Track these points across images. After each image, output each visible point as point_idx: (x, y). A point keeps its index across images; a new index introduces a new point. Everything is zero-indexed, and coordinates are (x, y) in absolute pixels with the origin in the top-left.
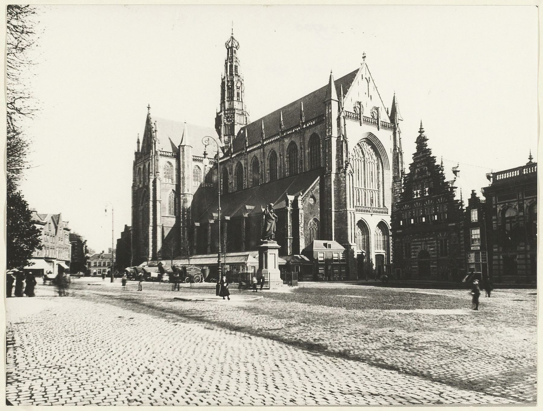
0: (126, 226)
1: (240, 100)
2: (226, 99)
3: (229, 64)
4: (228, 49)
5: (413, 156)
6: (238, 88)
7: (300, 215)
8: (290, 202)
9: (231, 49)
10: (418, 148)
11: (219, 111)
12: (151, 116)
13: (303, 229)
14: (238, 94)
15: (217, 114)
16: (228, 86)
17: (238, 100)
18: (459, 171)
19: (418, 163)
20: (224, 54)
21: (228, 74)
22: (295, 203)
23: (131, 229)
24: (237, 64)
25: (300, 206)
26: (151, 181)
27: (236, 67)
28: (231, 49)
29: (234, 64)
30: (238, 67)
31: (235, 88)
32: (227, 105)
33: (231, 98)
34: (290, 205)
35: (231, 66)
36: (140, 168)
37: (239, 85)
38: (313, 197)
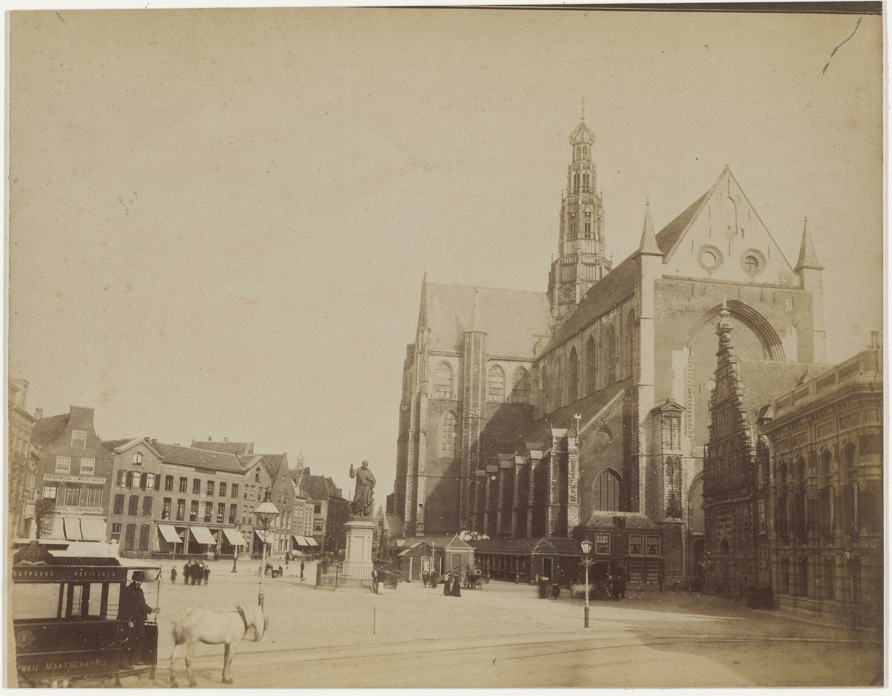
1: (592, 236)
3: (573, 173)
4: (574, 146)
6: (588, 215)
7: (570, 464)
8: (555, 441)
9: (581, 147)
12: (428, 280)
13: (576, 490)
14: (587, 226)
17: (587, 237)
20: (566, 155)
21: (572, 191)
22: (564, 442)
24: (588, 172)
25: (572, 445)
27: (586, 177)
28: (581, 147)
29: (583, 172)
31: (581, 215)
34: (555, 446)
35: (577, 177)
38: (605, 429)
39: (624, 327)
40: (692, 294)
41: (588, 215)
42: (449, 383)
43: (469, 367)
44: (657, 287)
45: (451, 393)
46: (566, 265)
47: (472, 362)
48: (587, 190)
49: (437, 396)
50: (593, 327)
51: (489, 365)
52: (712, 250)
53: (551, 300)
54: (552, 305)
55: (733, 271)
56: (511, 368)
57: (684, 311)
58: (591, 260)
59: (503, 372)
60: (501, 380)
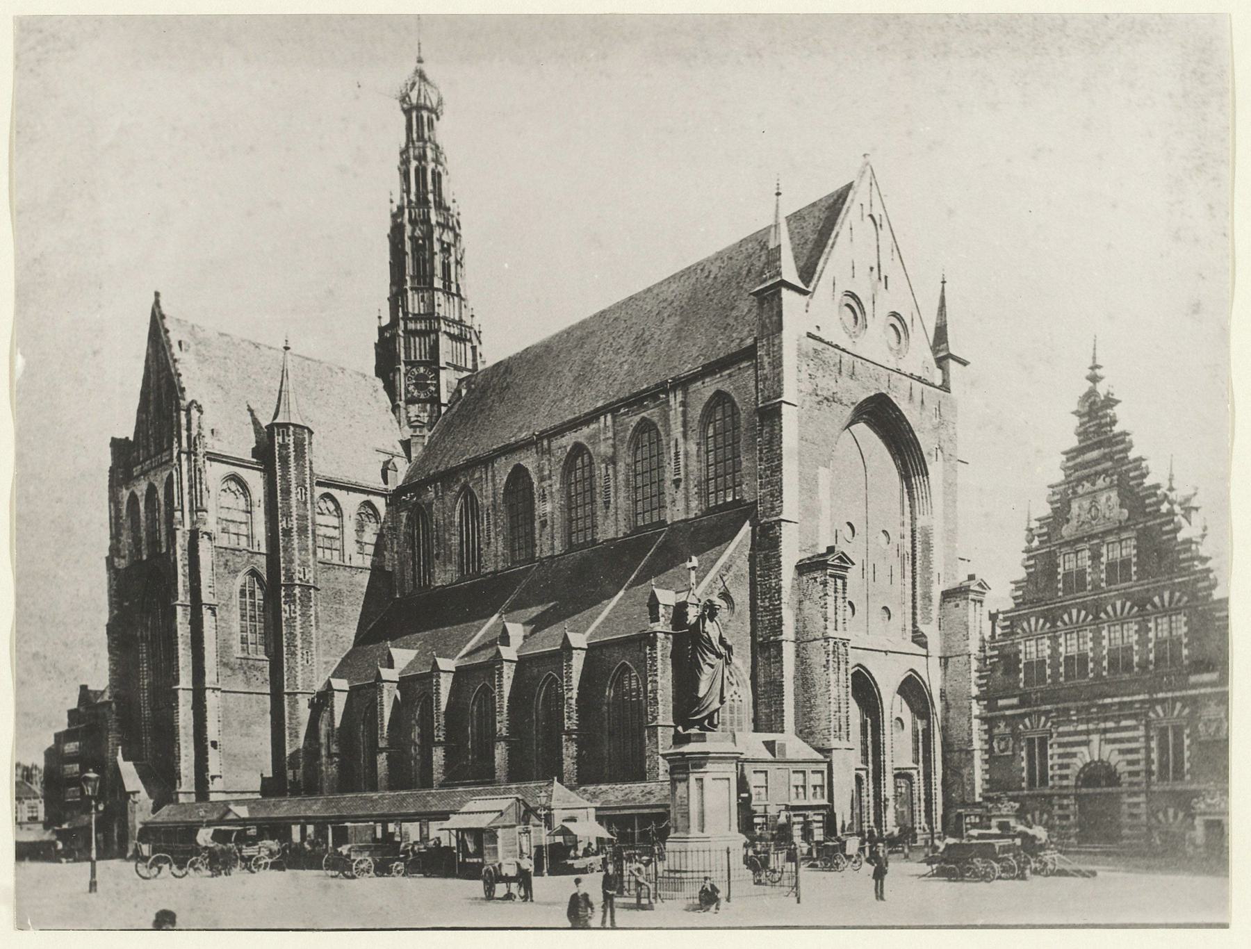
0: (84, 688)
1: (454, 290)
2: (409, 285)
5: (1064, 458)
10: (1083, 434)
11: (386, 321)
15: (382, 330)
16: (412, 238)
17: (446, 290)
18: (1197, 509)
19: (1079, 481)
23: (106, 697)
26: (181, 541)
30: (444, 179)
31: (437, 247)
32: (414, 303)
33: (424, 282)
36: (133, 499)
37: (448, 237)
39: (694, 424)
40: (840, 372)
41: (446, 250)
42: (242, 517)
43: (287, 492)
44: (801, 354)
45: (250, 537)
46: (416, 333)
47: (293, 482)
48: (441, 206)
49: (223, 541)
50: (586, 430)
51: (319, 491)
52: (854, 303)
53: (391, 388)
54: (393, 400)
55: (875, 342)
56: (351, 502)
57: (831, 399)
58: (455, 331)
59: (338, 507)
60: (335, 521)
